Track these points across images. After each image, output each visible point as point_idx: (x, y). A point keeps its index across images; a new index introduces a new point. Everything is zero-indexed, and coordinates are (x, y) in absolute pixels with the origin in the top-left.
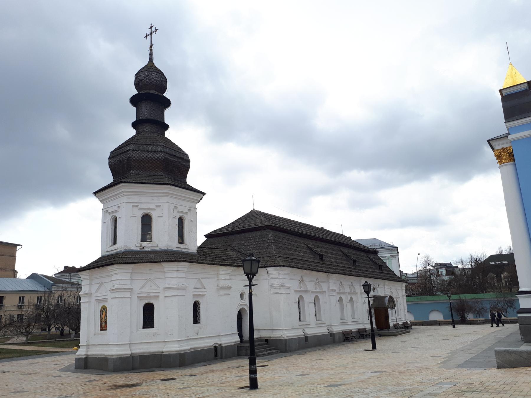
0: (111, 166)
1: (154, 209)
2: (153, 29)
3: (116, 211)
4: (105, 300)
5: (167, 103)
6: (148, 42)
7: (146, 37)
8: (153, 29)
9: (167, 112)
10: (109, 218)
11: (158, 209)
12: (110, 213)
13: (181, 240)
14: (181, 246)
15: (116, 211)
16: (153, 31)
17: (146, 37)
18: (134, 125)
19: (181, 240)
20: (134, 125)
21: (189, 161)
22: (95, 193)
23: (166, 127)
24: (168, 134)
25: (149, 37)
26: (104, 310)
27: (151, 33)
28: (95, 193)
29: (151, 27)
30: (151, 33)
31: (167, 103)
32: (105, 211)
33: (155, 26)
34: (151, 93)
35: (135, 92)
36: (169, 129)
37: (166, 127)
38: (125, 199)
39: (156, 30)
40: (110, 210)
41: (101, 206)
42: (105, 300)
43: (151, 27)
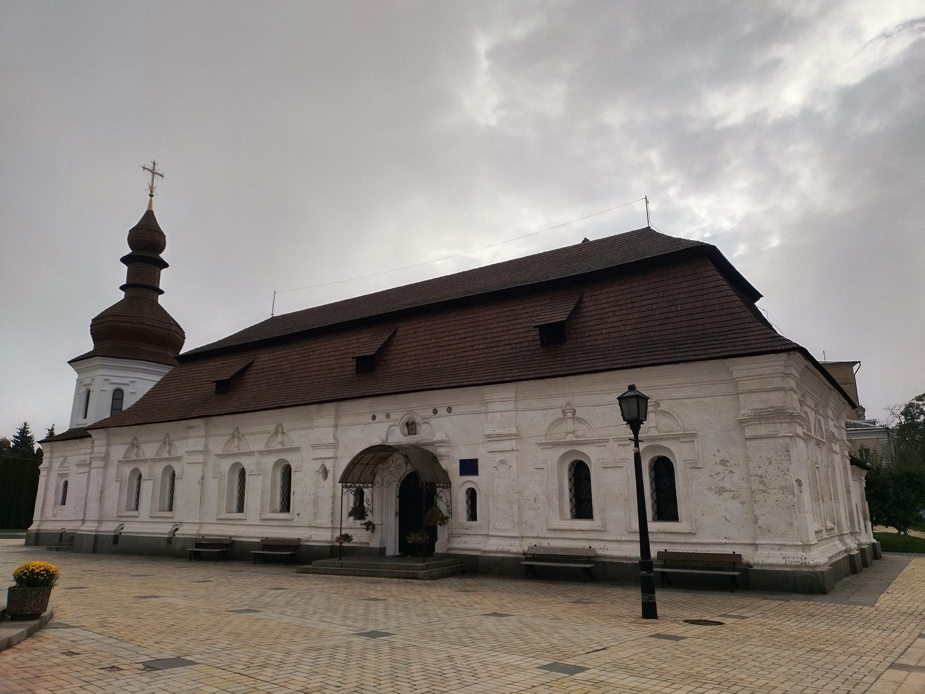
0: (93, 333)
1: (127, 385)
3: (90, 384)
4: (67, 475)
10: (84, 389)
11: (132, 384)
12: (85, 385)
15: (90, 384)
18: (123, 288)
20: (123, 288)
22: (69, 362)
26: (66, 483)
28: (69, 362)
32: (79, 382)
35: (129, 251)
37: (162, 292)
38: (101, 372)
40: (88, 381)
41: (76, 376)
42: (67, 475)
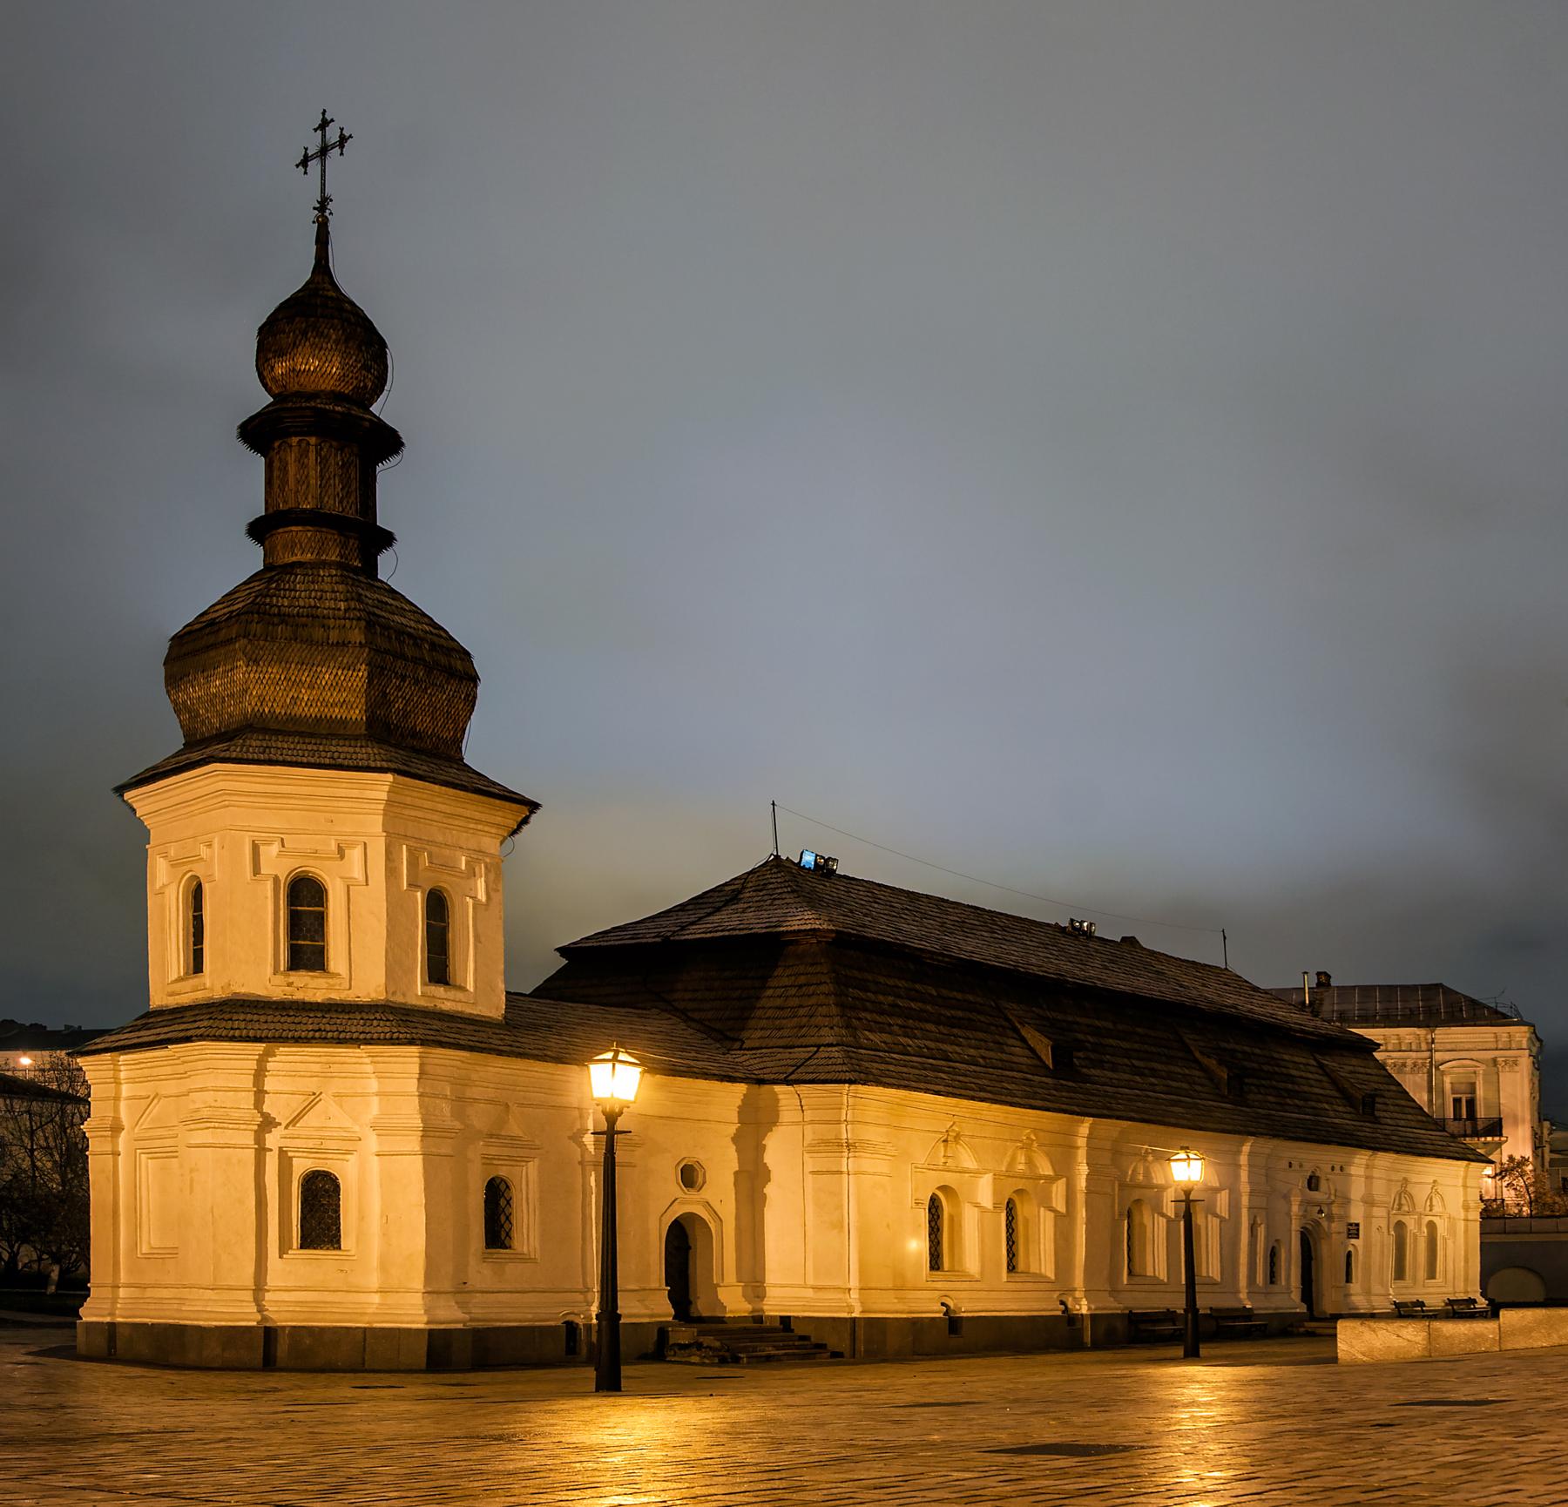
2: (333, 135)
5: (387, 442)
6: (307, 187)
7: (304, 162)
8: (333, 135)
9: (388, 475)
13: (439, 971)
14: (439, 991)
16: (328, 144)
17: (304, 162)
19: (439, 971)
21: (474, 679)
23: (387, 539)
24: (388, 567)
25: (314, 165)
27: (324, 151)
29: (324, 124)
30: (324, 151)
31: (387, 442)
33: (342, 121)
34: (326, 405)
36: (396, 546)
37: (387, 539)
39: (343, 140)
43: (324, 124)
